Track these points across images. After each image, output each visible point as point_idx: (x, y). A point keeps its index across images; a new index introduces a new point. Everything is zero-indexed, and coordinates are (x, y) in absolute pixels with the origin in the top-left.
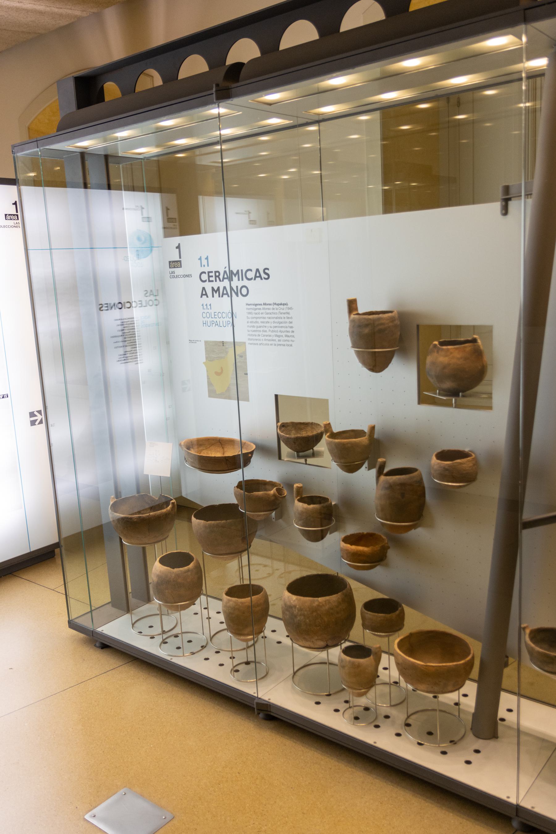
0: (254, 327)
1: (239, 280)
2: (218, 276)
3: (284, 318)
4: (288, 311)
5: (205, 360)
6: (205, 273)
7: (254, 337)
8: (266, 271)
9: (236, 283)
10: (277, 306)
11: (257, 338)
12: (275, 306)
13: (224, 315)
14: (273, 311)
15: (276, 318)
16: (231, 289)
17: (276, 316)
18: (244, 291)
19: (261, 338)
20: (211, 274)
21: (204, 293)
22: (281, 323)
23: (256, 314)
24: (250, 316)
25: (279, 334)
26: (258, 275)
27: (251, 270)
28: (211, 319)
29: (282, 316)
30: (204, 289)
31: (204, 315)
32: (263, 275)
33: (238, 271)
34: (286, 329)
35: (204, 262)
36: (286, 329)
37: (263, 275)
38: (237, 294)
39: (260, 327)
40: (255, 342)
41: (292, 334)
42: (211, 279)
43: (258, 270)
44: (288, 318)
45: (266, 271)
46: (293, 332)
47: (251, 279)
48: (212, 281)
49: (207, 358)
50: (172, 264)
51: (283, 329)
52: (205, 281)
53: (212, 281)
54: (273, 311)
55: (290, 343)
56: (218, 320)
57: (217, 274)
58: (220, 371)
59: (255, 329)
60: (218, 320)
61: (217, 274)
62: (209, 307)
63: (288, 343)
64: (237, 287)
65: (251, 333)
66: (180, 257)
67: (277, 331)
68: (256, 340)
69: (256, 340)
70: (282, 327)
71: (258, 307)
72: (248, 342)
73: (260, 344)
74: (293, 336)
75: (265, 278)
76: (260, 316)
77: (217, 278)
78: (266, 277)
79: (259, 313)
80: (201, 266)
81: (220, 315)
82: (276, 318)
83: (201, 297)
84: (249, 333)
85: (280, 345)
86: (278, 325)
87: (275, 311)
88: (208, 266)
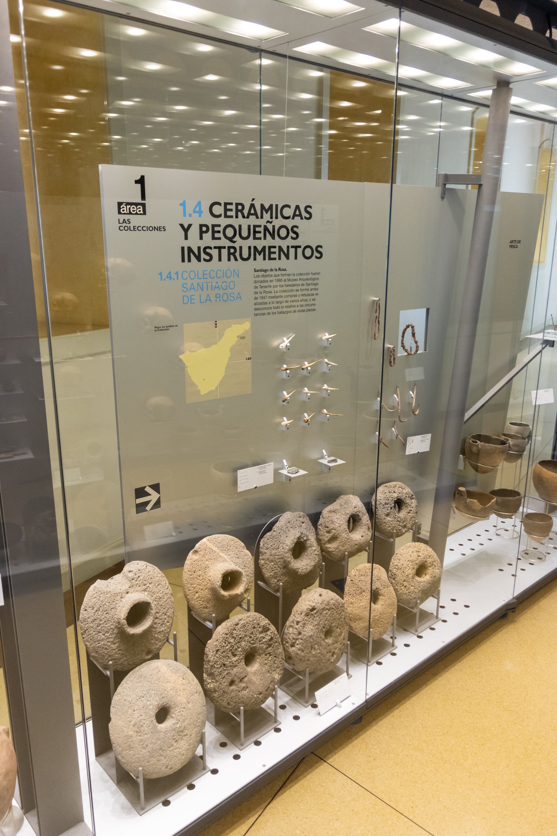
2: (241, 211)
6: (219, 204)
8: (308, 209)
20: (229, 207)
26: (297, 213)
27: (289, 206)
32: (304, 214)
33: (271, 206)
37: (304, 214)
42: (229, 213)
43: (297, 207)
45: (308, 209)
48: (232, 217)
52: (220, 216)
53: (232, 217)
61: (240, 207)
75: (306, 218)
77: (239, 214)
78: (308, 216)
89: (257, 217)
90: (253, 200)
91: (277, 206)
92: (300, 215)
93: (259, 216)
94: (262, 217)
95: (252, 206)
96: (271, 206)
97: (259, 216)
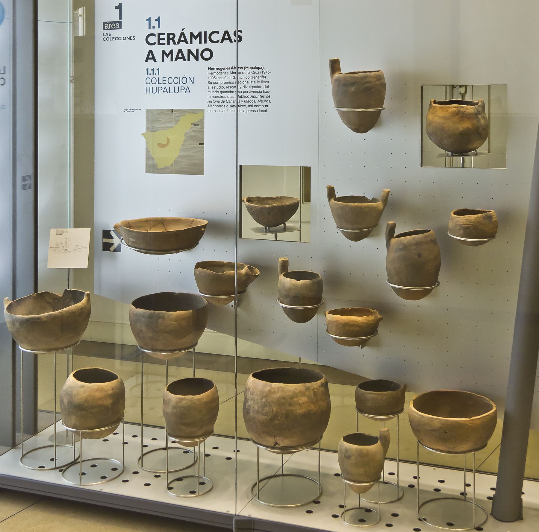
0: (217, 92)
1: (200, 42)
2: (173, 39)
3: (258, 82)
4: (264, 75)
5: (144, 131)
6: (154, 35)
7: (217, 104)
9: (195, 46)
10: (249, 70)
11: (220, 104)
12: (247, 70)
13: (177, 80)
14: (244, 75)
15: (248, 83)
16: (190, 52)
17: (247, 80)
18: (207, 54)
19: (225, 104)
20: (161, 37)
21: (150, 56)
22: (254, 87)
23: (221, 78)
24: (212, 81)
25: (252, 99)
27: (218, 32)
28: (157, 85)
29: (256, 80)
30: (151, 52)
31: (149, 81)
32: (233, 37)
34: (260, 94)
35: (154, 23)
36: (260, 94)
38: (197, 58)
39: (225, 92)
40: (218, 109)
41: (268, 99)
42: (161, 41)
43: (226, 32)
44: (263, 82)
46: (269, 96)
47: (218, 41)
48: (164, 44)
49: (147, 128)
50: (108, 26)
51: (256, 94)
52: (154, 44)
53: (164, 44)
54: (244, 75)
55: (264, 108)
56: (168, 86)
57: (171, 36)
58: (165, 143)
59: (219, 95)
60: (168, 86)
62: (156, 72)
63: (261, 109)
64: (197, 50)
65: (212, 99)
66: (120, 18)
67: (248, 97)
68: (219, 106)
69: (219, 106)
70: (254, 92)
71: (223, 71)
72: (206, 109)
73: (224, 111)
74: (269, 102)
76: (227, 80)
77: (171, 41)
79: (225, 78)
80: (150, 28)
81: (171, 81)
82: (248, 83)
83: (146, 61)
84: (209, 99)
85: (251, 111)
86: (249, 90)
87: (247, 75)
88: (159, 27)
89: (187, 43)
90: (183, 29)
91: (205, 33)
92: (230, 39)
93: (189, 41)
94: (191, 43)
95: (182, 34)
96: (200, 34)
97: (189, 41)
